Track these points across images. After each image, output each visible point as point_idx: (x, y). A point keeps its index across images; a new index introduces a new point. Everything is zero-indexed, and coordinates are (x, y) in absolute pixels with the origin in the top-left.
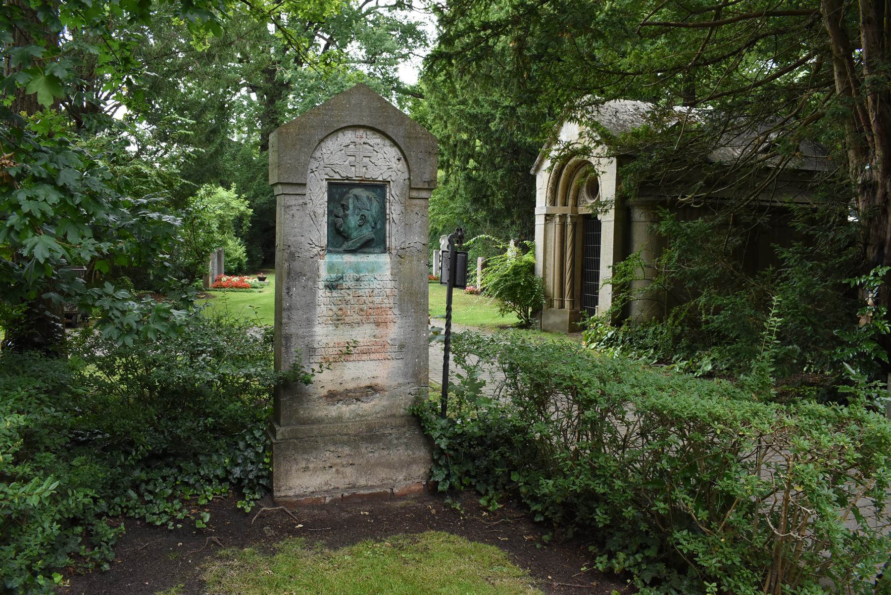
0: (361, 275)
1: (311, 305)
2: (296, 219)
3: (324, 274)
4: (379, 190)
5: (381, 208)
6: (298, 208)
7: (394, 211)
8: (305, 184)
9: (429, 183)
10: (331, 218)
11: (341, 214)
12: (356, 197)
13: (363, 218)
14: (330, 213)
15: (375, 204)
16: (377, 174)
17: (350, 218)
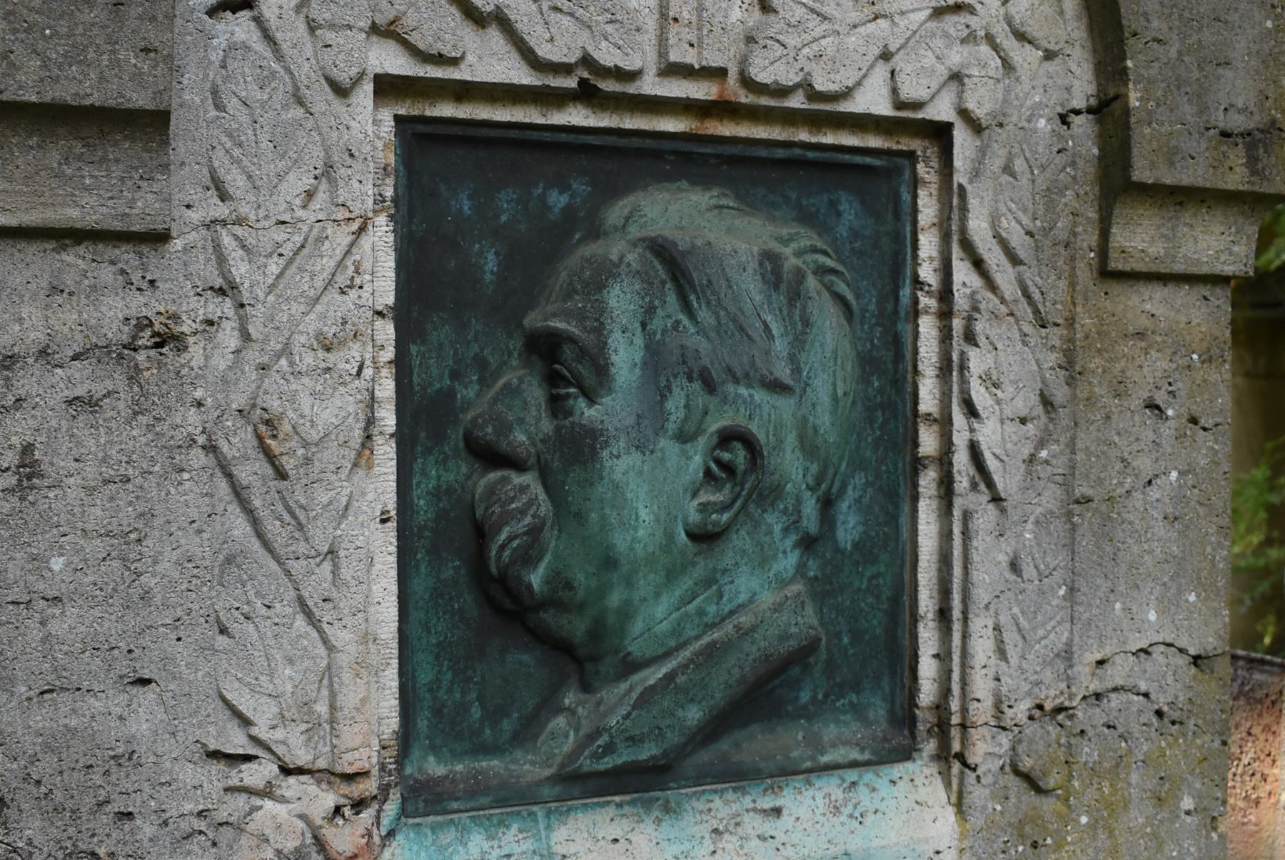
2: (66, 496)
4: (850, 211)
5: (867, 363)
6: (82, 378)
7: (993, 392)
8: (152, 125)
9: (1256, 142)
10: (431, 475)
11: (529, 426)
12: (674, 266)
13: (737, 461)
14: (424, 421)
17: (622, 465)
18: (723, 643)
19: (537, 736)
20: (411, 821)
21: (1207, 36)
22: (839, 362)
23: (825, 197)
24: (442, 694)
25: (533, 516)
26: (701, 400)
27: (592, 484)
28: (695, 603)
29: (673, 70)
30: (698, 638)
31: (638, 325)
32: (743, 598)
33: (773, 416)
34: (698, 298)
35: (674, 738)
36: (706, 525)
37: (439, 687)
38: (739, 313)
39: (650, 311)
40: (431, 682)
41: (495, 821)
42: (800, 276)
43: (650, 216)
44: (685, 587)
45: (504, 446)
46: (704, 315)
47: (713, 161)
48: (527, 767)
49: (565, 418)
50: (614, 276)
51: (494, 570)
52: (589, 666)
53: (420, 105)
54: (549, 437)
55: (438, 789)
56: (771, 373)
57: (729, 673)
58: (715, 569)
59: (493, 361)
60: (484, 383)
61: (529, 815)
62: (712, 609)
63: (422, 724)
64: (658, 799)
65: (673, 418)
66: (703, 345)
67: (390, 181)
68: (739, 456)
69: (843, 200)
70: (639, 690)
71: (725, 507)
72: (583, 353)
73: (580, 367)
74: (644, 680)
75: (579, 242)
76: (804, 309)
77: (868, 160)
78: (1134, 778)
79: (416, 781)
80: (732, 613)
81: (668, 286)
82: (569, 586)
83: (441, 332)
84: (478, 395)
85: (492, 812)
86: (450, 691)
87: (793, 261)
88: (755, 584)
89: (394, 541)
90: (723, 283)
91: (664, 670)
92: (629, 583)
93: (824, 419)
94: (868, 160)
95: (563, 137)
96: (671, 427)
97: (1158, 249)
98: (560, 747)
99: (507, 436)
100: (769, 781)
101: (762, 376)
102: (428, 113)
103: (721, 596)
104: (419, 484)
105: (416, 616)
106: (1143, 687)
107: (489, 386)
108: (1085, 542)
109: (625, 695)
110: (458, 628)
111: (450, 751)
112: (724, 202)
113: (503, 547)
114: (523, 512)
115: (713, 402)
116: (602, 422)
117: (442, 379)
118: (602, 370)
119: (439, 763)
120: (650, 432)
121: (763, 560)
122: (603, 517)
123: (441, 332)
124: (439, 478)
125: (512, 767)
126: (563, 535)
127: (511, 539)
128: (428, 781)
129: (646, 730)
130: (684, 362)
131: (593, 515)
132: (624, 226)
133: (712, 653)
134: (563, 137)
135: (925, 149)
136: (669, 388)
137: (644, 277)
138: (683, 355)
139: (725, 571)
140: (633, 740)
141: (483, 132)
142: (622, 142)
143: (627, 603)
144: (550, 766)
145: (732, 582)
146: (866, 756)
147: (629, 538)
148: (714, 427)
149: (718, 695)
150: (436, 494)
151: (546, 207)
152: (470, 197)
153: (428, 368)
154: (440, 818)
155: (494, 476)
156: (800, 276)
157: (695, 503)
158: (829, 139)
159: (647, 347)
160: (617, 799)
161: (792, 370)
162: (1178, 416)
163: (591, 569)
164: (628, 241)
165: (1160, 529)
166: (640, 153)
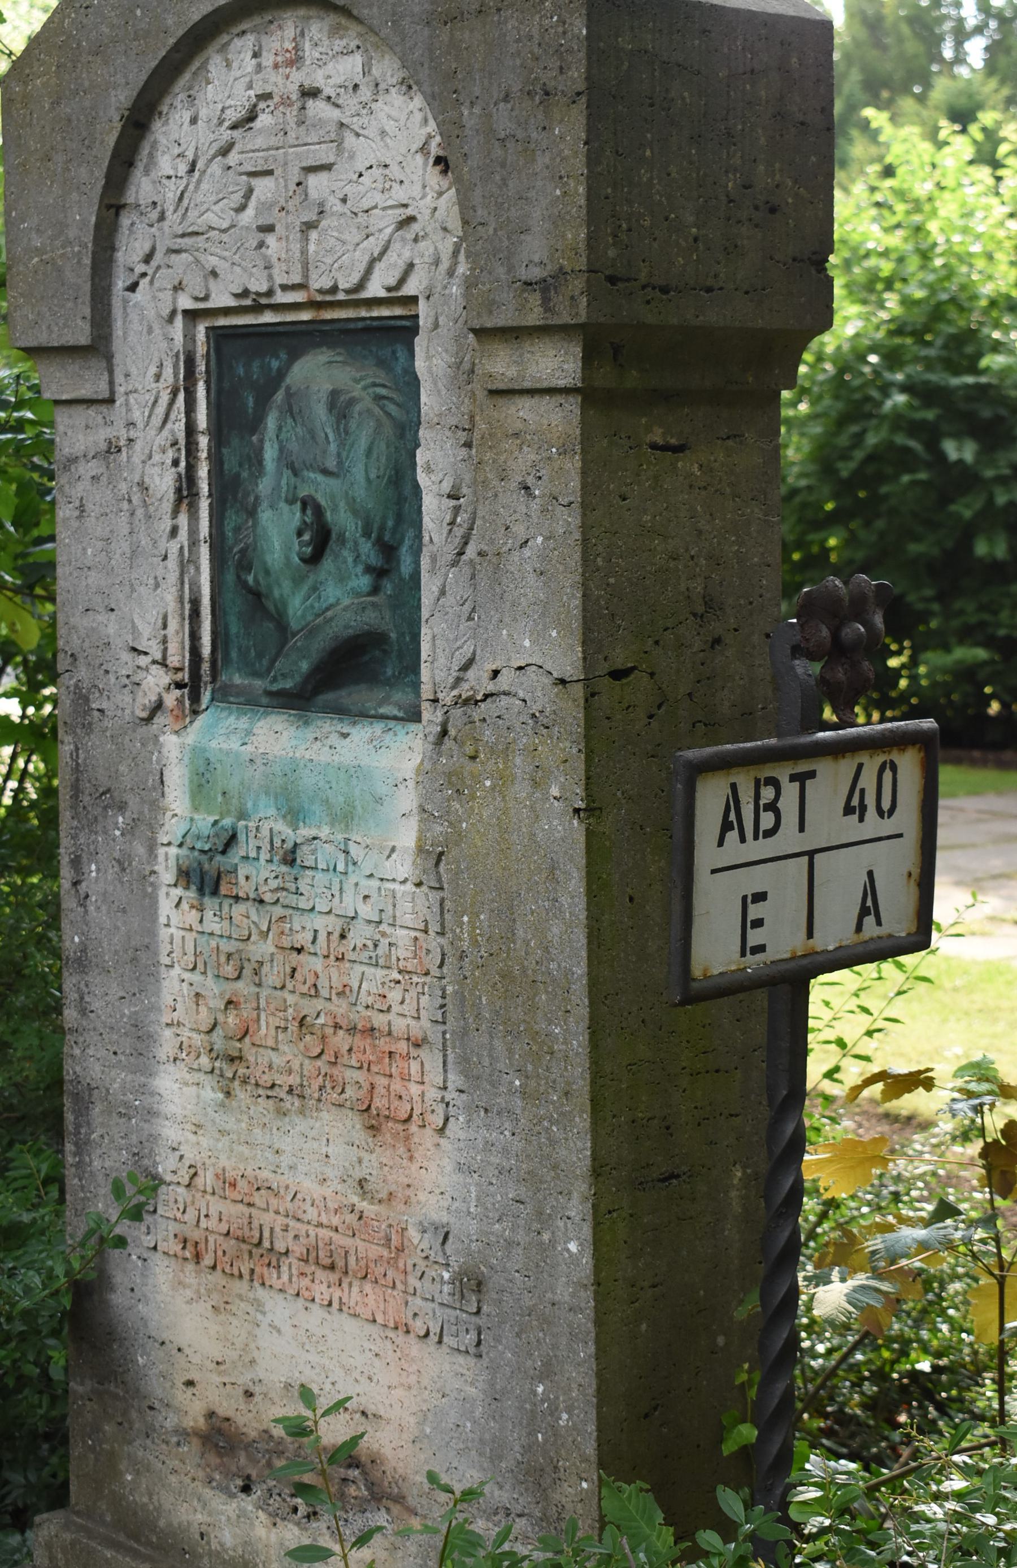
0: (305, 832)
1: (141, 962)
3: (180, 815)
16: (345, 260)
21: (513, 213)
22: (375, 455)
26: (293, 480)
29: (285, 288)
32: (332, 600)
76: (346, 425)
78: (518, 761)
88: (338, 593)
97: (512, 372)
106: (521, 694)
108: (483, 584)
121: (342, 579)
141: (245, 330)
146: (401, 714)
158: (375, 313)
162: (544, 495)
165: (531, 578)
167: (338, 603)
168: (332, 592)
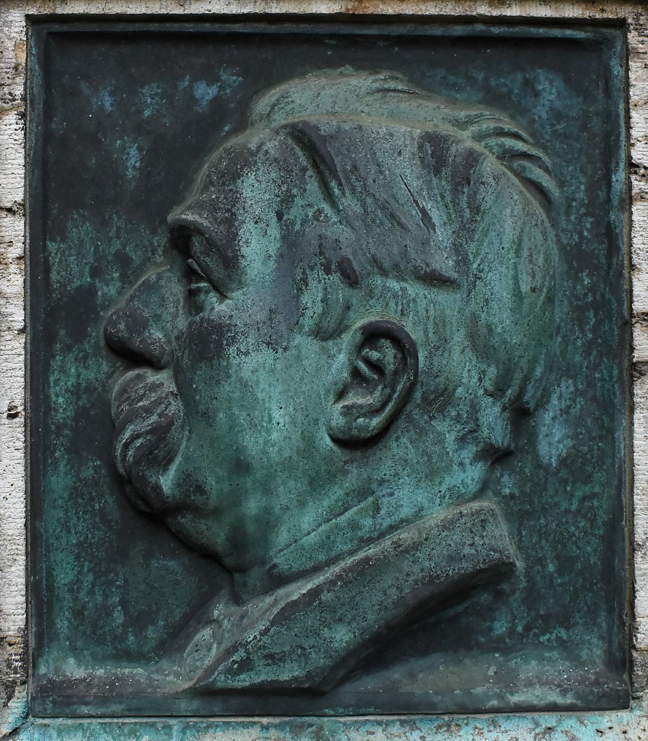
4: (550, 90)
5: (575, 258)
11: (165, 325)
13: (387, 359)
15: (510, 213)
17: (251, 362)
18: (378, 560)
19: (183, 647)
20: (40, 721)
22: (525, 253)
23: (519, 76)
24: (82, 595)
25: (160, 416)
26: (342, 293)
27: (218, 383)
28: (347, 515)
30: (351, 553)
31: (273, 215)
32: (406, 512)
33: (432, 312)
34: (340, 184)
35: (319, 661)
36: (350, 429)
37: (79, 589)
38: (392, 201)
39: (287, 200)
40: (72, 583)
41: (126, 731)
42: (472, 159)
43: (298, 102)
44: (334, 497)
45: (136, 343)
46: (350, 203)
47: (381, 43)
48: (171, 678)
49: (197, 314)
50: (247, 164)
51: (121, 470)
52: (237, 576)
53: (51, 4)
54: (183, 334)
55: (69, 692)
56: (428, 265)
57: (385, 594)
58: (370, 479)
59: (136, 257)
60: (125, 279)
61: (164, 727)
62: (367, 522)
63: (62, 624)
64: (311, 725)
65: (309, 313)
66: (345, 234)
67: (20, 80)
68: (388, 354)
69: (542, 78)
70: (281, 605)
71: (374, 412)
72: (210, 245)
73: (207, 259)
74: (288, 595)
75: (230, 134)
76: (473, 195)
77: (569, 33)
79: (50, 681)
80: (392, 528)
81: (309, 173)
82: (200, 489)
83: (81, 229)
84: (119, 293)
85: (127, 720)
86: (91, 593)
87: (469, 144)
88: (421, 498)
89: (22, 436)
90: (373, 169)
91: (310, 586)
92: (266, 489)
93: (502, 317)
94: (569, 33)
95: (207, 27)
96: (308, 322)
98: (201, 659)
99: (140, 333)
100: (446, 718)
101: (415, 267)
102: (59, 11)
103: (378, 509)
104: (57, 382)
105: (53, 516)
107: (131, 284)
109: (267, 610)
110: (99, 529)
111: (92, 654)
112: (392, 85)
113: (126, 446)
114: (148, 411)
115: (357, 296)
116: (231, 316)
117: (82, 276)
118: (231, 262)
119: (79, 665)
120: (283, 328)
121: (432, 472)
122: (232, 418)
123: (81, 229)
124: (79, 376)
125: (156, 676)
126: (193, 435)
127: (134, 438)
128: (62, 682)
129: (287, 648)
130: (321, 253)
131: (221, 415)
132: (269, 115)
133: (364, 572)
134: (207, 27)
135: (637, 17)
136: (305, 281)
137: (283, 164)
138: (320, 245)
139: (381, 482)
140: (272, 659)
141: (121, 27)
142: (273, 28)
143: (268, 510)
144: (191, 679)
145: (392, 494)
146: (569, 700)
147: (261, 441)
148: (359, 324)
149: (371, 617)
150: (76, 392)
151: (193, 100)
152: (111, 94)
153: (68, 266)
154: (70, 722)
155: (131, 374)
156: (472, 159)
157: (340, 405)
159: (284, 238)
160: (265, 720)
161: (457, 263)
163: (221, 473)
164: (272, 129)
166: (295, 39)
167: (419, 514)
168: (406, 497)
